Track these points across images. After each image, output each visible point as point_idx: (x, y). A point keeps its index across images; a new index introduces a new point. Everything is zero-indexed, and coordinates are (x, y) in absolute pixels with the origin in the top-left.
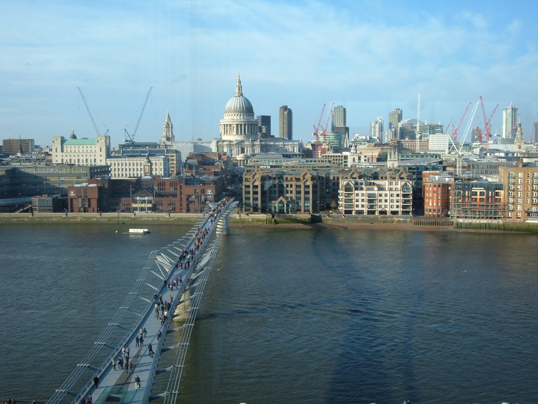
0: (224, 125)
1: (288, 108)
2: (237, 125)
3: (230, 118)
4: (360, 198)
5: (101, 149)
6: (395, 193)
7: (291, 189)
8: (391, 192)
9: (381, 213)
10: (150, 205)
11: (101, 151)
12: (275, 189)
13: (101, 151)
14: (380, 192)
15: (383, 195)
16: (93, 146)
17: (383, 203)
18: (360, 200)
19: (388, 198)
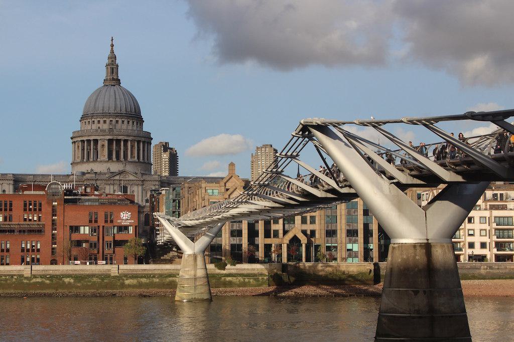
0: (83, 141)
1: (170, 146)
2: (110, 142)
3: (95, 127)
18: (477, 233)
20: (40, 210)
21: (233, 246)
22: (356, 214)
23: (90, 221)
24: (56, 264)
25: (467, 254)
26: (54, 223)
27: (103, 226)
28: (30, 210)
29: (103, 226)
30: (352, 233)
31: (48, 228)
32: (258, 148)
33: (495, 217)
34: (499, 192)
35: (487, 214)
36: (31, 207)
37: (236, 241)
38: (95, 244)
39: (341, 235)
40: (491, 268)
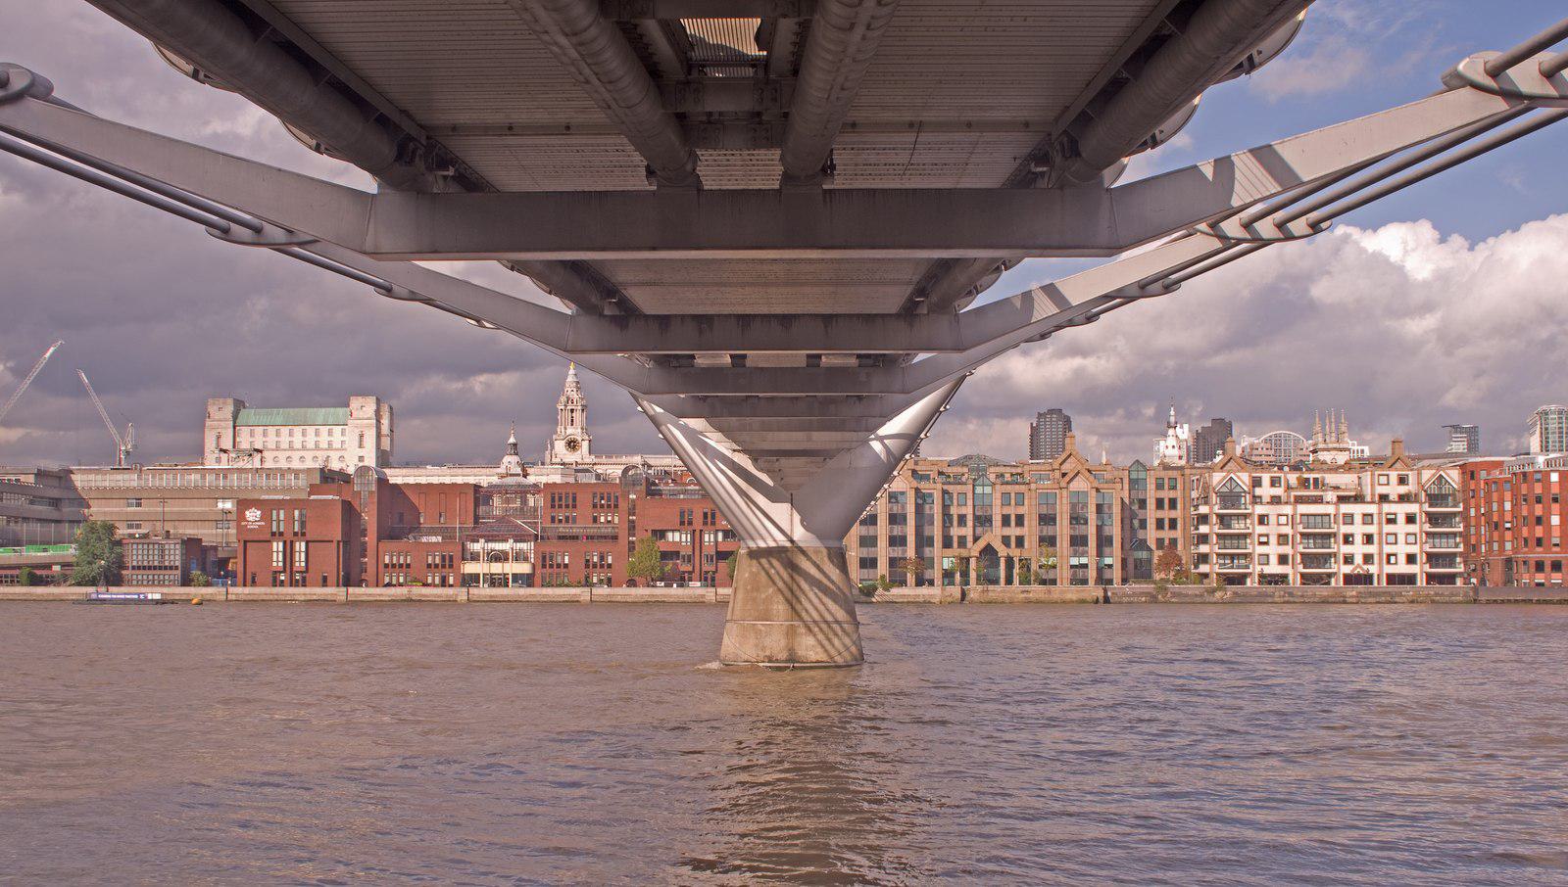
4: (1272, 530)
5: (361, 436)
6: (1402, 510)
7: (1021, 510)
8: (1386, 508)
9: (1349, 579)
10: (524, 568)
11: (361, 446)
12: (963, 511)
13: (361, 446)
14: (1345, 508)
15: (1358, 519)
16: (337, 430)
17: (1358, 549)
18: (1273, 540)
19: (1372, 529)
20: (616, 506)
21: (893, 562)
22: (1085, 510)
23: (682, 523)
24: (635, 586)
25: (1257, 573)
26: (632, 528)
27: (701, 531)
28: (602, 506)
29: (701, 531)
30: (1078, 541)
31: (623, 533)
32: (1040, 415)
33: (1302, 515)
34: (1312, 476)
35: (1288, 509)
36: (603, 502)
37: (897, 552)
38: (689, 556)
39: (1063, 543)
40: (1291, 594)
